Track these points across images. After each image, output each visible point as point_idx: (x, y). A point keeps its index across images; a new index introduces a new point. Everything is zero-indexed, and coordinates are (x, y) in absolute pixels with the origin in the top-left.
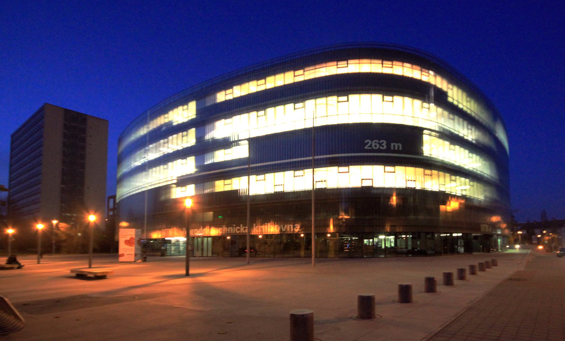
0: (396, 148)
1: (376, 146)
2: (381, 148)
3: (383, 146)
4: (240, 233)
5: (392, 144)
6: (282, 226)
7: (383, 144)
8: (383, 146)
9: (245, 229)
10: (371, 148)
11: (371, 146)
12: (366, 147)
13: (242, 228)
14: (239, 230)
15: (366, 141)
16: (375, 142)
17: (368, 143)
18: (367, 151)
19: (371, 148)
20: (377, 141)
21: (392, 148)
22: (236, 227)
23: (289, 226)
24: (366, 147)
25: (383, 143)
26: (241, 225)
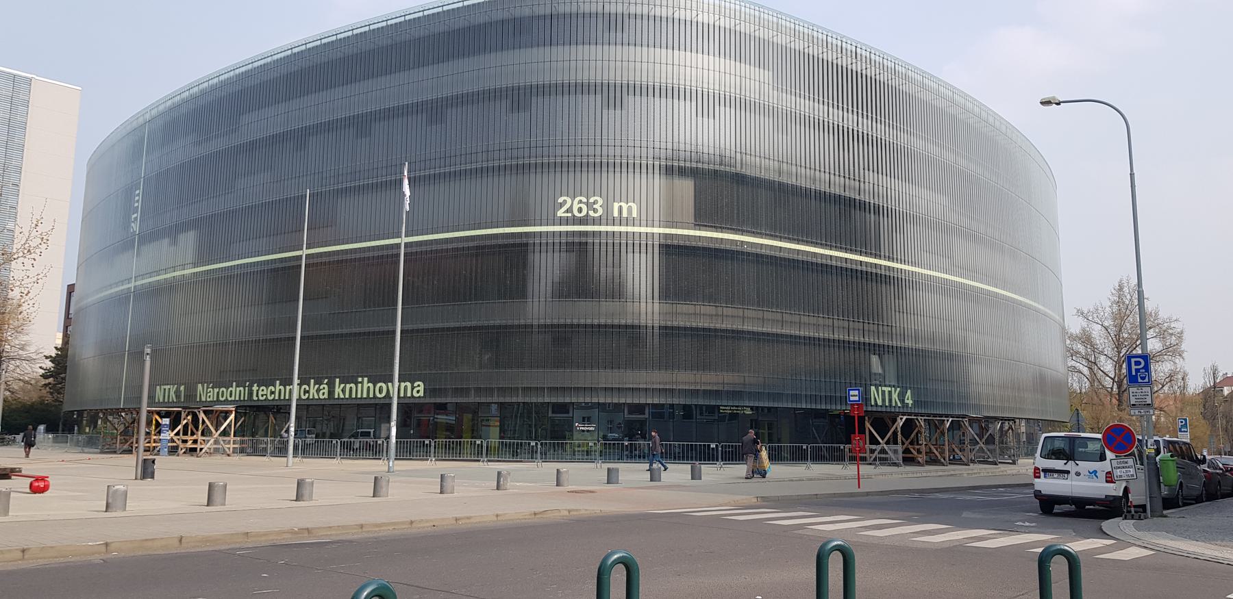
0: (625, 214)
1: (580, 210)
2: (591, 213)
3: (595, 211)
4: (308, 398)
5: (616, 205)
7: (595, 206)
8: (595, 211)
9: (318, 391)
10: (570, 215)
11: (567, 211)
12: (560, 213)
13: (315, 385)
14: (308, 392)
15: (560, 200)
16: (580, 202)
17: (565, 202)
18: (561, 222)
19: (570, 215)
20: (584, 200)
21: (616, 214)
24: (560, 213)
25: (594, 203)
26: (312, 381)
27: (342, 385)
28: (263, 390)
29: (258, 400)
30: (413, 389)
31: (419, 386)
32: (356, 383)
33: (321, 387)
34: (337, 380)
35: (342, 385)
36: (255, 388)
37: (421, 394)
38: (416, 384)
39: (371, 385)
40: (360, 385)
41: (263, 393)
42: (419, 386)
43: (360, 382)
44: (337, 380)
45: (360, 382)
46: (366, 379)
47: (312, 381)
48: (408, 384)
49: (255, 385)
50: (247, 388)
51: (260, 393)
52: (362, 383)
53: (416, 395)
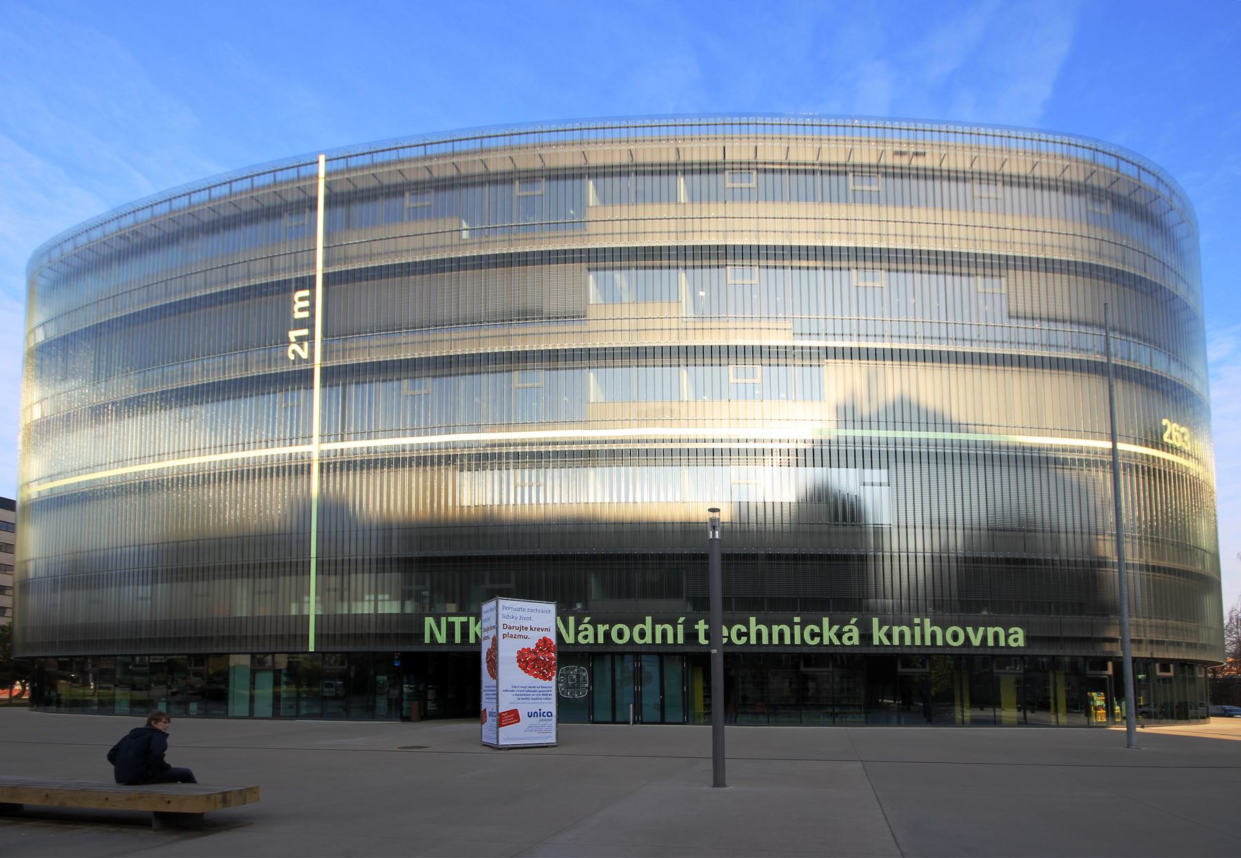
6: (970, 630)
9: (839, 635)
14: (820, 635)
23: (991, 631)
27: (885, 628)
30: (1007, 636)
31: (1016, 633)
32: (911, 626)
33: (846, 628)
34: (875, 621)
35: (885, 628)
37: (1021, 643)
39: (938, 630)
40: (917, 630)
42: (1016, 633)
43: (918, 625)
44: (875, 621)
45: (918, 625)
46: (927, 621)
52: (922, 625)
53: (1012, 644)
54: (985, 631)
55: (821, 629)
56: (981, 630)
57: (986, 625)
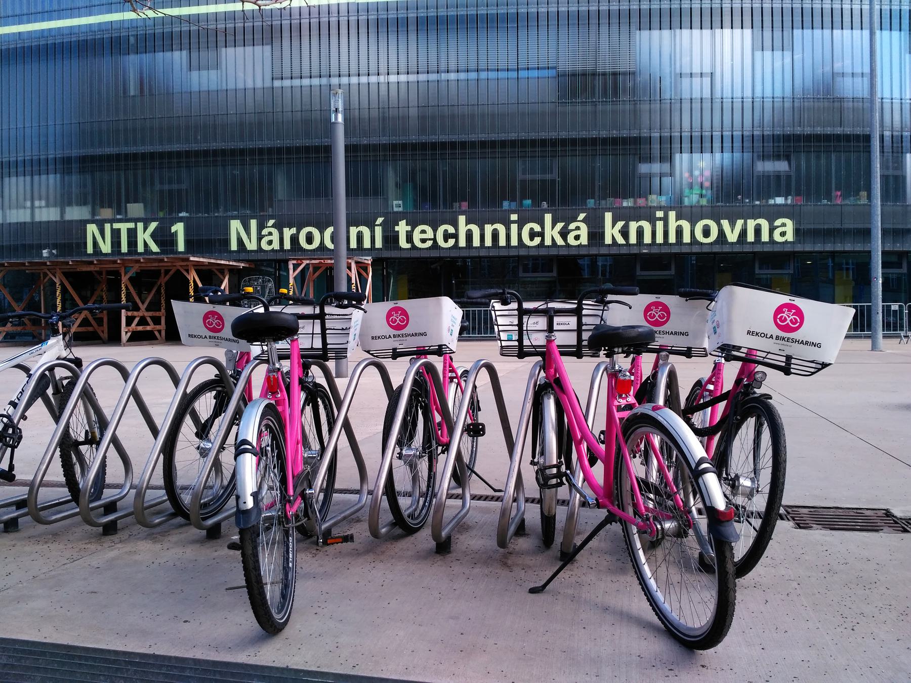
6: (725, 223)
13: (553, 225)
14: (542, 235)
22: (521, 224)
23: (751, 224)
27: (620, 224)
28: (423, 232)
29: (414, 247)
31: (784, 225)
32: (653, 221)
33: (572, 226)
34: (608, 216)
35: (620, 224)
36: (402, 228)
38: (778, 222)
39: (686, 225)
40: (660, 225)
41: (424, 236)
42: (784, 225)
43: (660, 219)
44: (608, 216)
45: (660, 219)
47: (548, 218)
48: (764, 224)
49: (403, 223)
50: (378, 231)
51: (417, 236)
52: (665, 220)
54: (745, 224)
55: (543, 228)
56: (740, 223)
57: (746, 218)
